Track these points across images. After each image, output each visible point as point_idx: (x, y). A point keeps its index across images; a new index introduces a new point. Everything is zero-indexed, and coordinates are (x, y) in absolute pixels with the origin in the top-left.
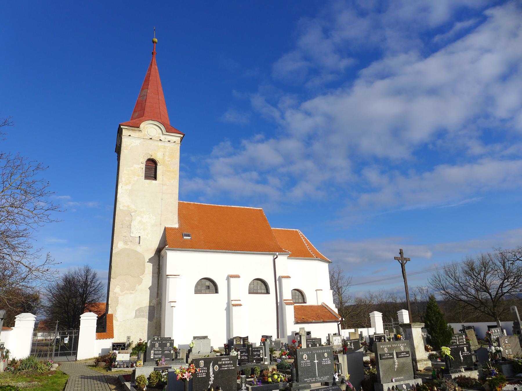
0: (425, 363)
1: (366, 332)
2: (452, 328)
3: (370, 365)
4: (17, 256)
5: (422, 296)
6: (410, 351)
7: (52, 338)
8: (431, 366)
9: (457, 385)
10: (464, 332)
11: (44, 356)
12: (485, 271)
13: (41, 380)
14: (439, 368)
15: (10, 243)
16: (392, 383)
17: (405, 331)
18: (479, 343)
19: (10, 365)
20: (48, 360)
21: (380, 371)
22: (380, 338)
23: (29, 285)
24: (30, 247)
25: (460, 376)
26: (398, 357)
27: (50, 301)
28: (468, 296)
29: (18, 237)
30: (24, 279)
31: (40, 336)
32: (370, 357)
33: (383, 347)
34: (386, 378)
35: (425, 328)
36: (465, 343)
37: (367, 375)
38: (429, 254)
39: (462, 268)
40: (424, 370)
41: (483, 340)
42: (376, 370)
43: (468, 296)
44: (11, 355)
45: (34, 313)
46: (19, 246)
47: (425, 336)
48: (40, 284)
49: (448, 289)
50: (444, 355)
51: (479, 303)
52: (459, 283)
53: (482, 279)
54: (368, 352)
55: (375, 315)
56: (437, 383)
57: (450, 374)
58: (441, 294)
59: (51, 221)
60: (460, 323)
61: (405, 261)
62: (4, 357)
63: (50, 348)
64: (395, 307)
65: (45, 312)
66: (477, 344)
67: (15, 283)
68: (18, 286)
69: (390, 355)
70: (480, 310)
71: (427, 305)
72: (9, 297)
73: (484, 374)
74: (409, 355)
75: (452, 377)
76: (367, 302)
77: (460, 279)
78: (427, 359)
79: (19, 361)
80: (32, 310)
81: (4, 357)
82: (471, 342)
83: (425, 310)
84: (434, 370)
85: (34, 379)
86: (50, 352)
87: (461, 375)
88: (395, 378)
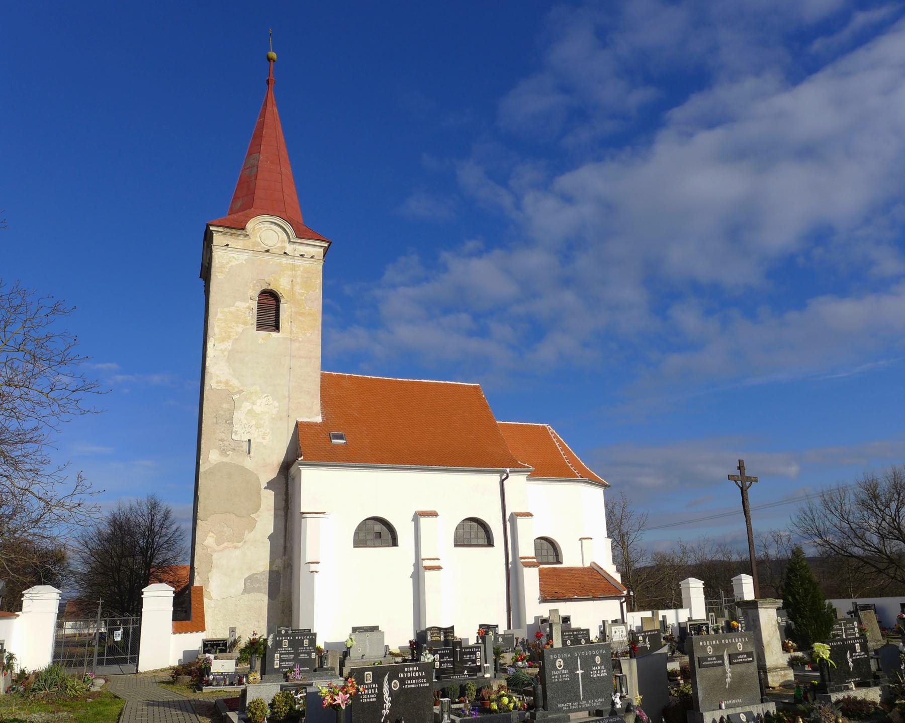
0: (783, 673)
1: (672, 617)
2: (833, 607)
3: (679, 678)
4: (22, 478)
5: (780, 549)
6: (754, 651)
7: (91, 631)
8: (793, 679)
9: (840, 714)
10: (857, 615)
11: (77, 665)
12: (898, 501)
13: (73, 710)
14: (809, 683)
15: (8, 455)
16: (720, 710)
17: (745, 615)
18: (883, 635)
19: (16, 681)
20: (85, 671)
21: (697, 689)
22: (698, 627)
23: (46, 534)
24: (45, 462)
25: (846, 697)
26: (732, 663)
27: (86, 562)
28: (866, 547)
29: (22, 442)
30: (37, 521)
31: (69, 628)
32: (680, 663)
33: (705, 644)
34: (709, 702)
35: (783, 608)
36: (857, 635)
37: (673, 696)
38: (793, 470)
39: (855, 495)
40: (780, 686)
41: (892, 630)
42: (691, 687)
43: (866, 547)
44: (17, 664)
45: (57, 586)
46: (26, 460)
47: (784, 624)
48: (66, 531)
49: (829, 534)
50: (818, 659)
51: (885, 561)
52: (849, 524)
53: (893, 516)
54: (677, 654)
55: (691, 585)
56: (804, 710)
57: (829, 694)
58: (816, 544)
59: (83, 412)
60: (849, 598)
61: (748, 483)
62: (4, 666)
63: (88, 651)
64: (728, 570)
65: (77, 583)
66: (881, 638)
67: (20, 530)
68: (25, 534)
69: (717, 660)
70: (887, 575)
71: (787, 565)
72: (10, 555)
73: (891, 694)
74: (753, 659)
75: (832, 699)
76: (676, 560)
77: (851, 515)
78: (786, 666)
79: (33, 674)
80: (53, 580)
81: (4, 666)
82: (868, 634)
83: (784, 576)
84: (798, 687)
85: (61, 707)
86: (89, 657)
87: (849, 696)
88: (725, 702)
